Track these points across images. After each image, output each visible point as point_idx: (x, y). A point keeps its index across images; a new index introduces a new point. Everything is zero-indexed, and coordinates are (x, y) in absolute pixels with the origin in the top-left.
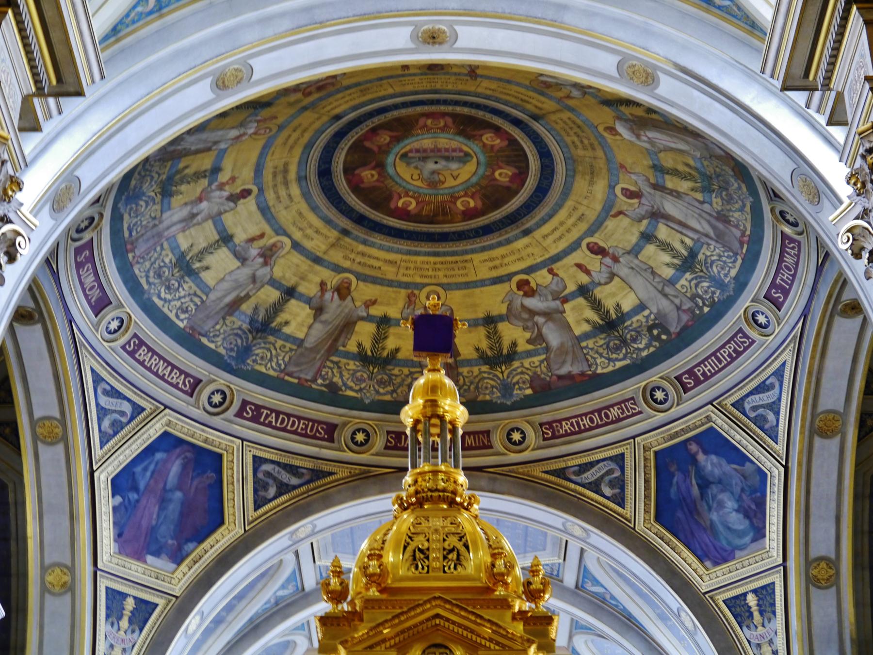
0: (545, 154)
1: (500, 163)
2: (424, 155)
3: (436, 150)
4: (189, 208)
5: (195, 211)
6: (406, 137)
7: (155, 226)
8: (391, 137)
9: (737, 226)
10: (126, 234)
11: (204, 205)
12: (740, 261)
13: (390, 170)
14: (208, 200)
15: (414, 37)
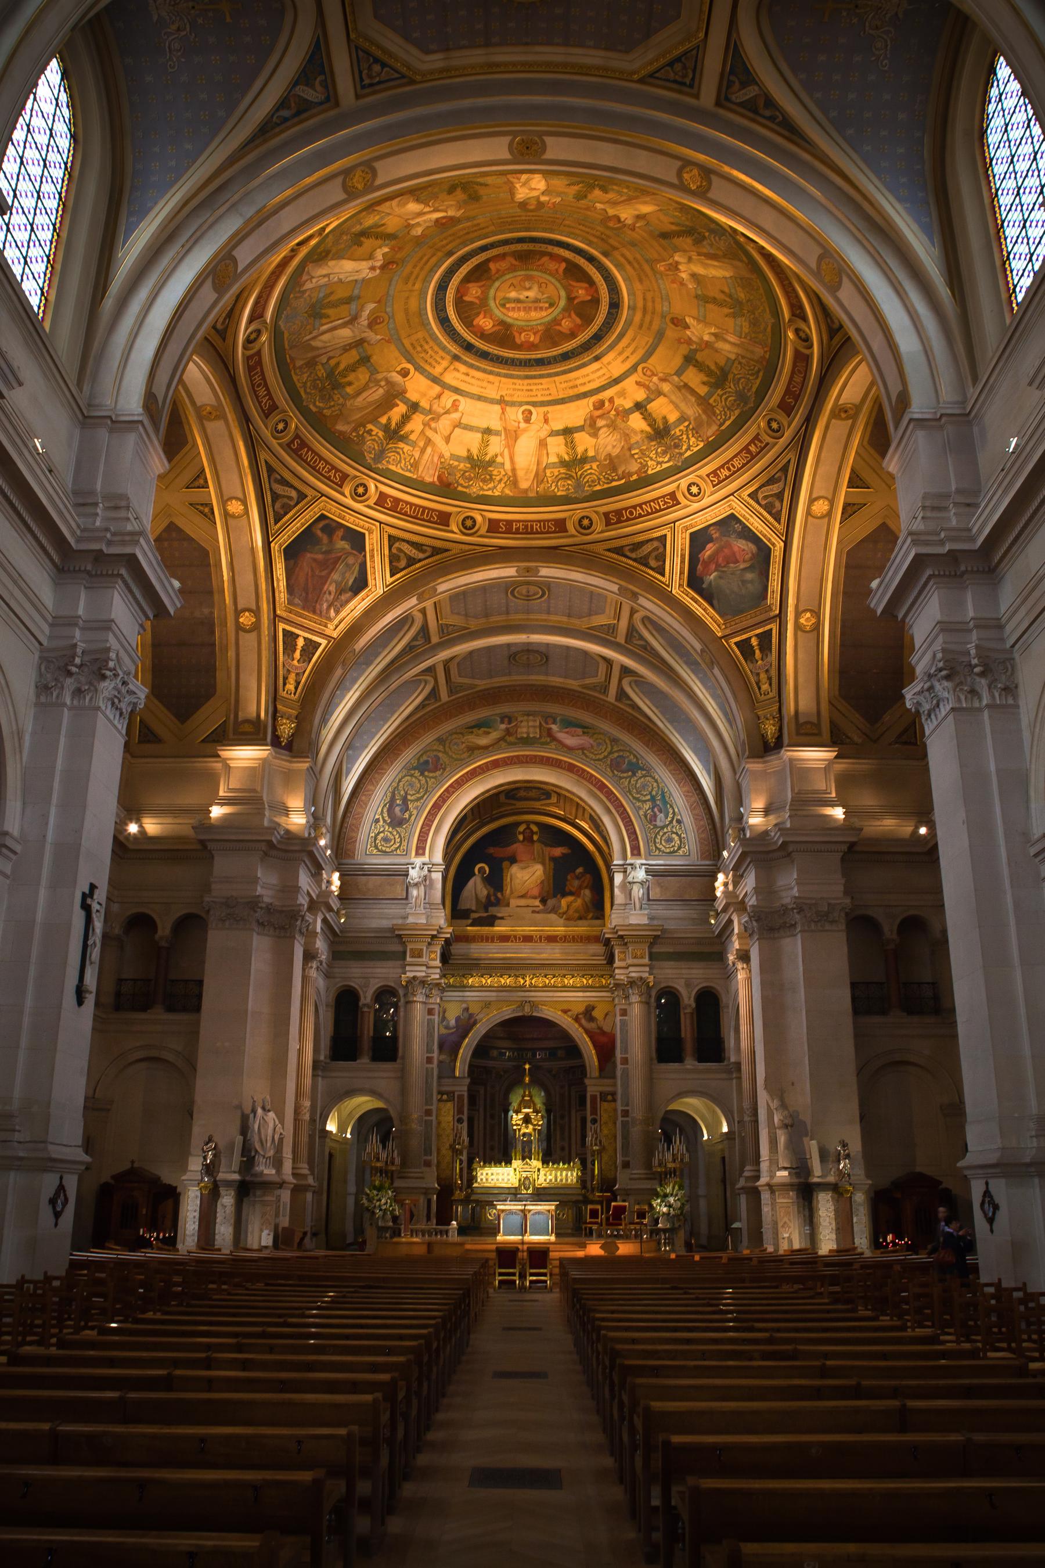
0: (444, 321)
1: (477, 301)
2: (536, 305)
3: (527, 310)
4: (716, 345)
5: (713, 339)
6: (549, 323)
7: (743, 357)
8: (560, 325)
9: (300, 367)
10: (761, 374)
11: (706, 338)
12: (287, 346)
13: (563, 293)
14: (702, 339)
15: (539, 571)
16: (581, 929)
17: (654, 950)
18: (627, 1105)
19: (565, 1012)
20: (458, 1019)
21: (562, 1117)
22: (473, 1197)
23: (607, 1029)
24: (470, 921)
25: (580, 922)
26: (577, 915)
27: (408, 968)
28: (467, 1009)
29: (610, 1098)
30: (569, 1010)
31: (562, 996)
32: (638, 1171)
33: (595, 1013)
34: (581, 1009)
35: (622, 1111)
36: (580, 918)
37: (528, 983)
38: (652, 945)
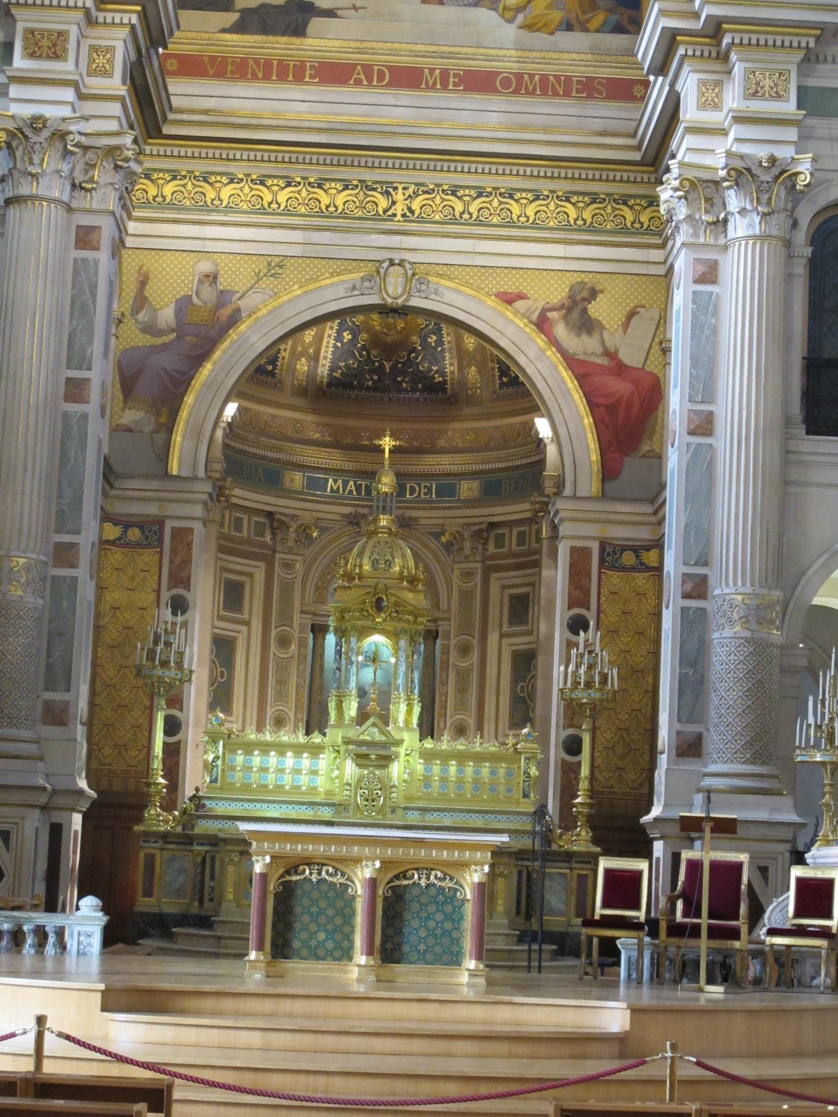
16: (575, 53)
17: (811, 82)
18: (704, 562)
19: (509, 299)
20: (183, 305)
21: (465, 650)
22: (203, 827)
23: (631, 357)
24: (232, 17)
25: (566, 39)
26: (557, 16)
27: (14, 91)
28: (212, 278)
29: (628, 558)
30: (521, 297)
31: (496, 275)
32: (722, 765)
33: (595, 309)
34: (557, 293)
35: (686, 577)
36: (569, 27)
37: (399, 209)
38: (811, 59)
